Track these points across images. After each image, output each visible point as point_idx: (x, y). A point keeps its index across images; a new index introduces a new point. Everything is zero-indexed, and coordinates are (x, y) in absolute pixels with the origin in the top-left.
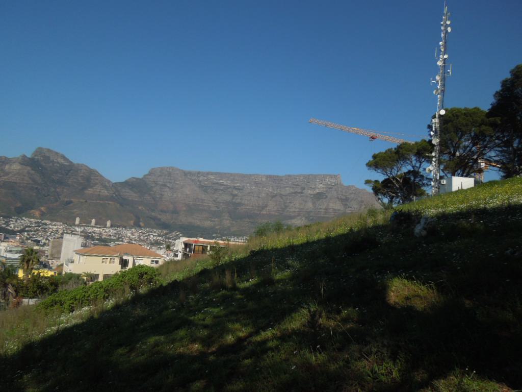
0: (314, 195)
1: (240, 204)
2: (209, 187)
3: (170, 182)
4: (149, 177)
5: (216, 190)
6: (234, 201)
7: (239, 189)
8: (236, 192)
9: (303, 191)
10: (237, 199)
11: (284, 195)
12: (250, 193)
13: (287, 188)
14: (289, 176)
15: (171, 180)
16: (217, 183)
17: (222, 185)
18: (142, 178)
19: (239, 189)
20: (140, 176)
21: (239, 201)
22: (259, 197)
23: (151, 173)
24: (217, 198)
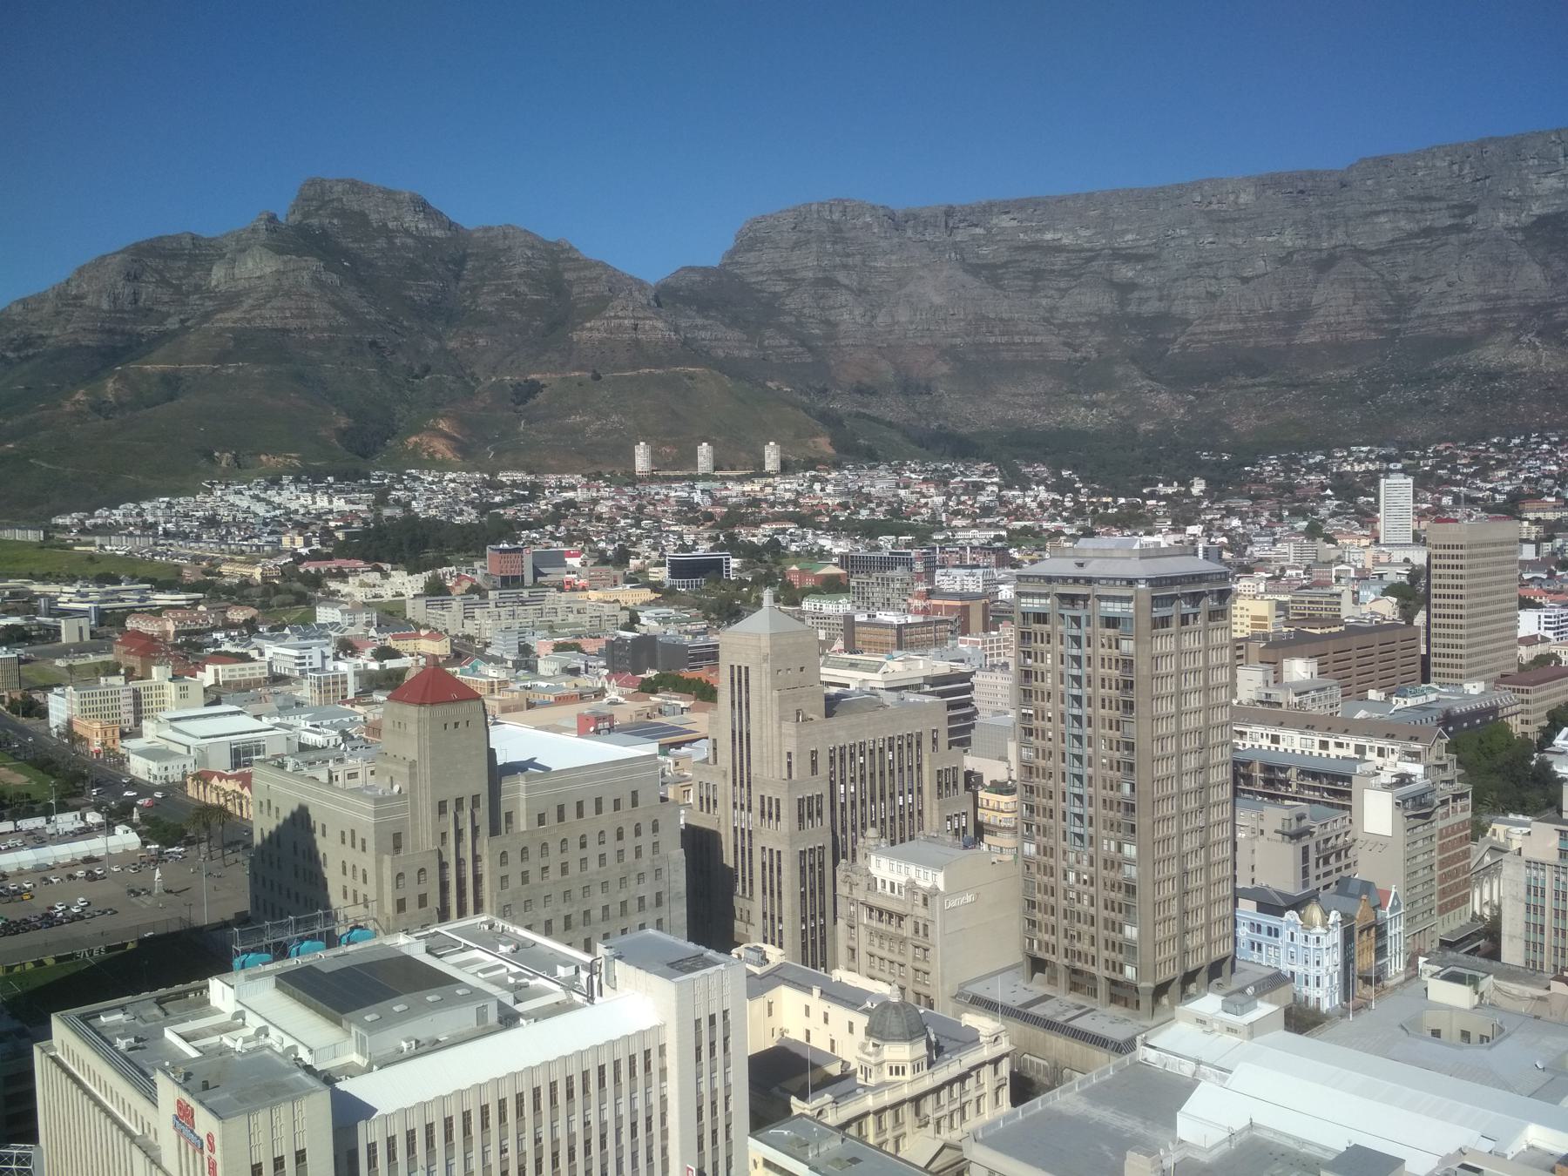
0: (1524, 229)
1: (1163, 319)
2: (1005, 265)
3: (845, 266)
4: (751, 257)
5: (1037, 275)
6: (1132, 309)
7: (1140, 258)
8: (1126, 272)
9: (1469, 220)
10: (1142, 301)
11: (1372, 253)
12: (1199, 265)
13: (1383, 219)
14: (1384, 161)
15: (848, 255)
16: (1034, 247)
17: (1058, 249)
18: (720, 271)
19: (1140, 258)
20: (713, 259)
21: (1152, 307)
22: (1245, 280)
23: (750, 241)
24: (1053, 309)
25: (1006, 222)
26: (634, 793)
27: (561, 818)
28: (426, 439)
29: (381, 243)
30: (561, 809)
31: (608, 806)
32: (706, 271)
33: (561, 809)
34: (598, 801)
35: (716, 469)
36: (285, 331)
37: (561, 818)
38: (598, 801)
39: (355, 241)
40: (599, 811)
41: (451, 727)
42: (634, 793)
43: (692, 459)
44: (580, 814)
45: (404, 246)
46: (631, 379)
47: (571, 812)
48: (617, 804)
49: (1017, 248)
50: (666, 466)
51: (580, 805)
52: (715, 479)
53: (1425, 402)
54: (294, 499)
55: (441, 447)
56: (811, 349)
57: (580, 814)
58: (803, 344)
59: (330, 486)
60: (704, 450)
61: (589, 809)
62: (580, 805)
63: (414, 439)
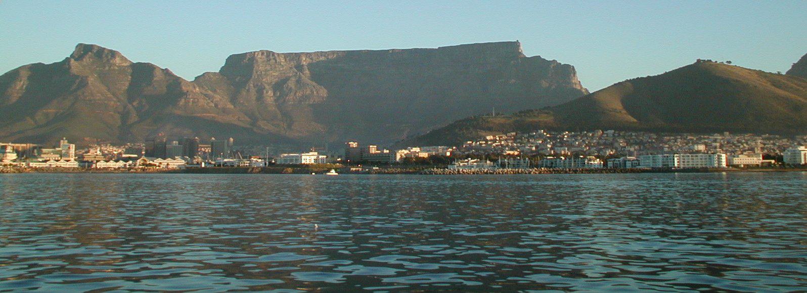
45: (114, 70)
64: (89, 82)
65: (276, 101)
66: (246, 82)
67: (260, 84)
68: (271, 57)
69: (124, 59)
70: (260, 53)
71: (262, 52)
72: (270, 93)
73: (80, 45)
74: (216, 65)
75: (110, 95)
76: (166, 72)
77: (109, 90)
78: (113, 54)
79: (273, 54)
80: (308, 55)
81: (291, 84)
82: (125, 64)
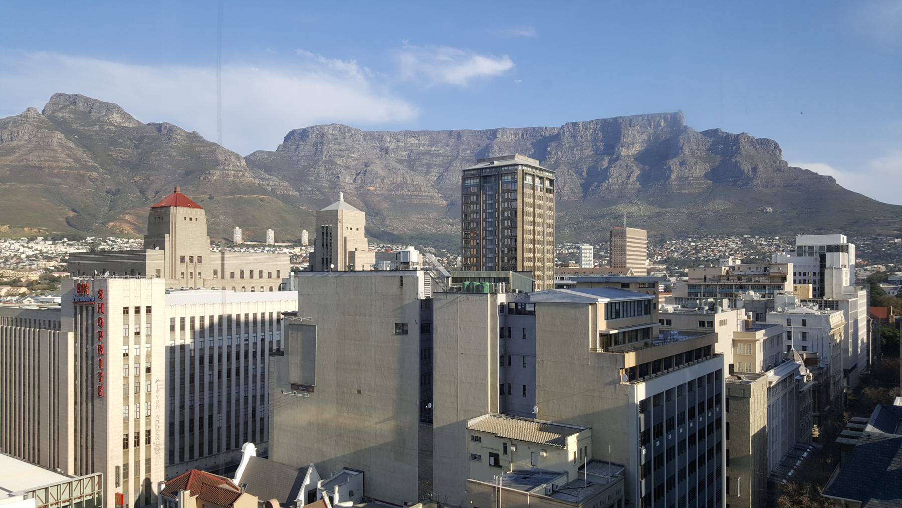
14: (575, 124)
16: (428, 153)
17: (438, 155)
25: (412, 141)
26: (278, 271)
27: (242, 277)
28: (118, 224)
29: (97, 128)
30: (242, 272)
31: (265, 275)
32: (269, 153)
33: (242, 272)
34: (261, 272)
35: (276, 242)
36: (40, 168)
37: (242, 277)
38: (261, 272)
39: (81, 126)
40: (261, 277)
41: (188, 219)
42: (278, 271)
43: (264, 238)
44: (252, 276)
46: (230, 200)
47: (247, 274)
48: (270, 275)
49: (419, 153)
50: (248, 240)
51: (251, 272)
52: (274, 246)
53: (594, 226)
54: (41, 246)
55: (126, 227)
56: (322, 193)
57: (252, 276)
58: (318, 190)
59: (65, 242)
60: (271, 233)
61: (256, 274)
62: (251, 272)
63: (111, 224)
64: (55, 140)
65: (358, 189)
66: (316, 163)
67: (333, 167)
68: (348, 134)
69: (125, 116)
70: (331, 128)
71: (335, 126)
72: (349, 179)
73: (59, 95)
74: (272, 143)
75: (91, 163)
76: (193, 137)
77: (95, 157)
78: (110, 108)
79: (349, 130)
80: (394, 136)
81: (378, 168)
82: (128, 124)
